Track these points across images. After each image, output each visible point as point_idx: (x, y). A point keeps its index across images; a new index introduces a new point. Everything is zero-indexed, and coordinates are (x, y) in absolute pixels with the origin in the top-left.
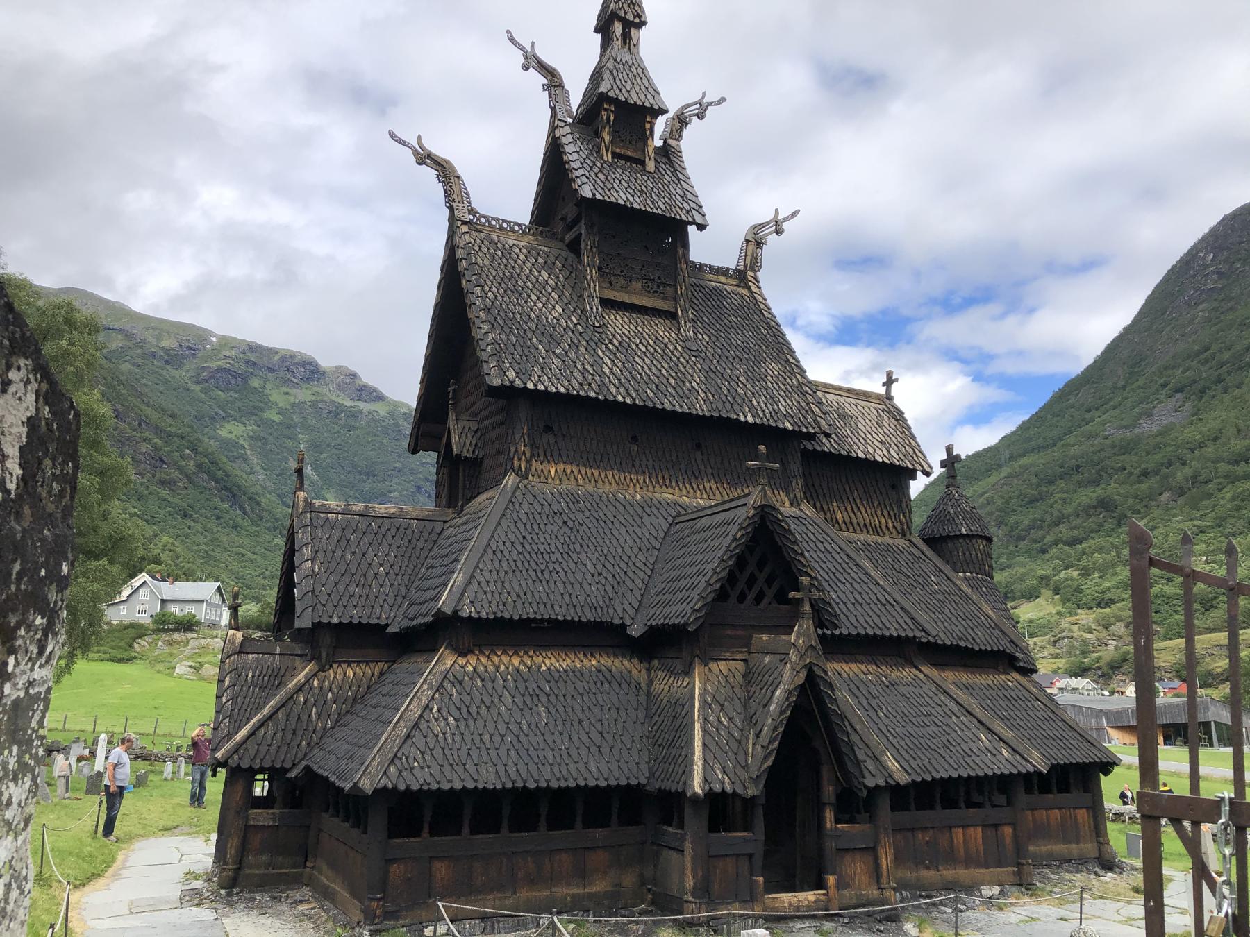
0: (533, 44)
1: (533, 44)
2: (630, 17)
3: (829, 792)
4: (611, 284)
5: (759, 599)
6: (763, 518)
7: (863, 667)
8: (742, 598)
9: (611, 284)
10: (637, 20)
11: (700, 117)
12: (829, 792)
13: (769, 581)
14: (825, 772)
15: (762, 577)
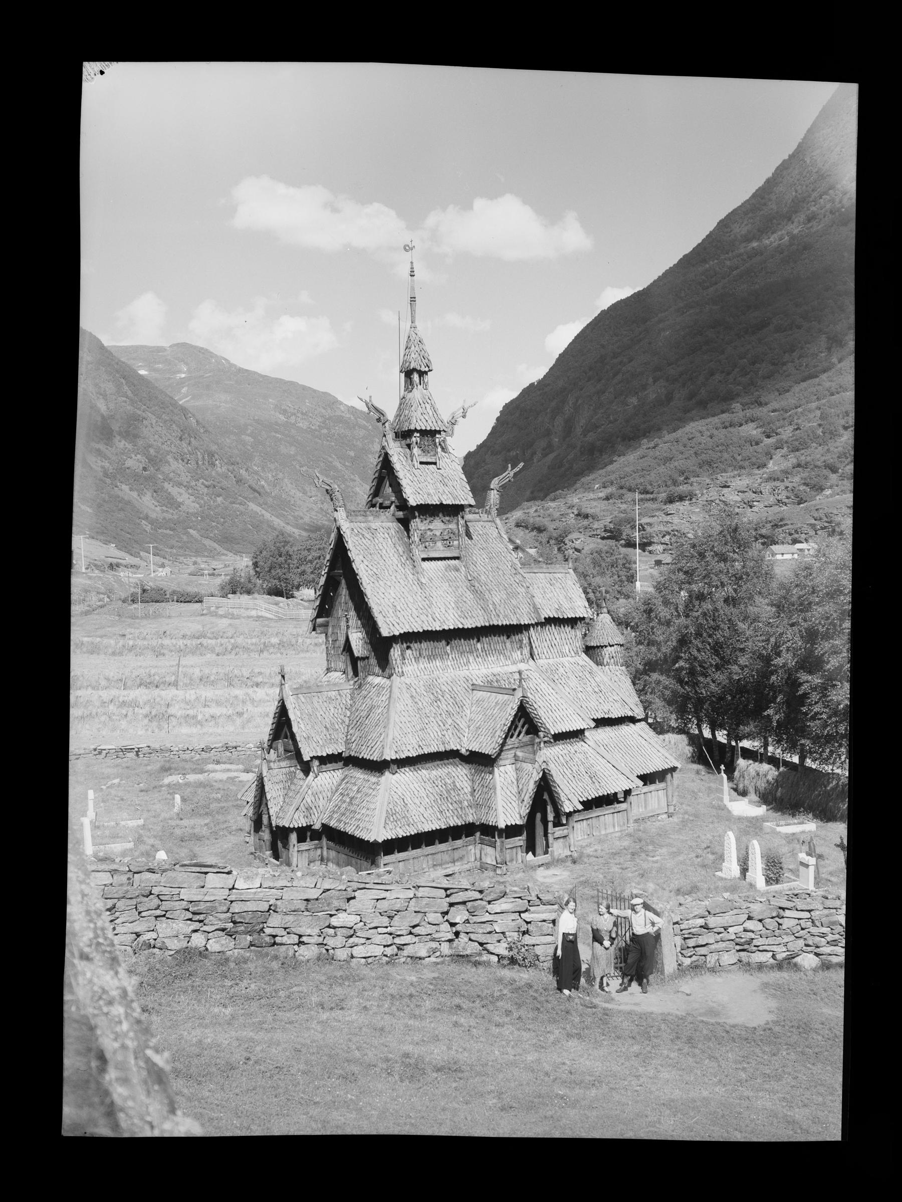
0: (370, 397)
1: (370, 397)
2: (423, 369)
3: (551, 817)
4: (426, 547)
5: (518, 735)
6: (522, 702)
7: (560, 747)
8: (511, 737)
9: (426, 547)
10: (427, 369)
11: (464, 417)
12: (551, 817)
13: (523, 727)
14: (549, 808)
15: (520, 725)
